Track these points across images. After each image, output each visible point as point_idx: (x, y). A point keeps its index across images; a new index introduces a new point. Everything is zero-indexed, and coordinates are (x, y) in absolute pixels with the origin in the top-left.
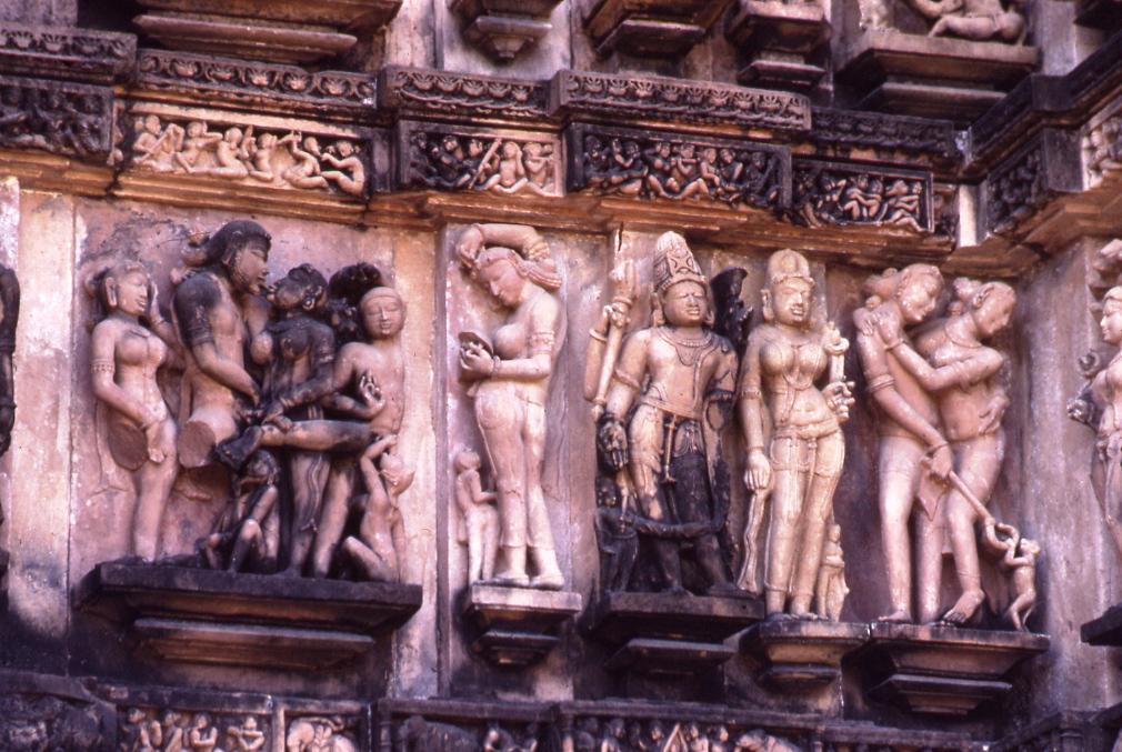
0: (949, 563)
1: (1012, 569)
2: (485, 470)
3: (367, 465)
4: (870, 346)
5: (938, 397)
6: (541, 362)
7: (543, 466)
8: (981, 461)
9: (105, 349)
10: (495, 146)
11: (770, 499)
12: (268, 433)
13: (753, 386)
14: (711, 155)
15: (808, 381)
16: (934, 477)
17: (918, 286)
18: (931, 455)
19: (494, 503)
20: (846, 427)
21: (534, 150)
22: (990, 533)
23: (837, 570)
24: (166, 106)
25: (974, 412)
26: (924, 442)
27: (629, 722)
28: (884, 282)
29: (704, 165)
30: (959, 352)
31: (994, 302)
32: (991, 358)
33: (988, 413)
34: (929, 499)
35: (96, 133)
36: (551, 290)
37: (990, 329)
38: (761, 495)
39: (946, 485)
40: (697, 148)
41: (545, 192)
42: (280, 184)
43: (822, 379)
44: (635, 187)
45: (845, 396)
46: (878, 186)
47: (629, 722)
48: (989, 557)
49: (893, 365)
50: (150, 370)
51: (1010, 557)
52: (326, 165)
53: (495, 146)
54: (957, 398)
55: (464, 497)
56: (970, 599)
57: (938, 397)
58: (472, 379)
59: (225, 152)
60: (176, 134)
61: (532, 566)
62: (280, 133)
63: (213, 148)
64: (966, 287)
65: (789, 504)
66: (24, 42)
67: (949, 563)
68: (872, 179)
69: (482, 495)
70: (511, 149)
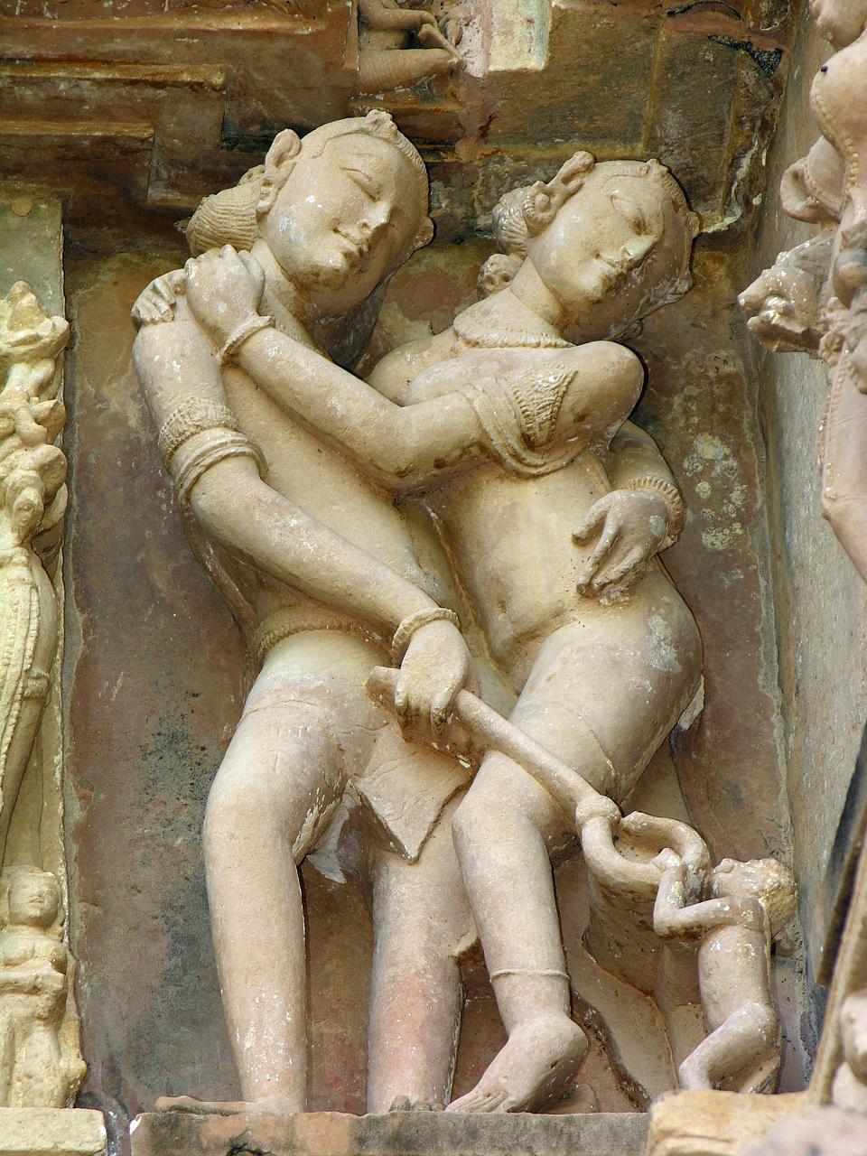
5: (431, 497)
8: (588, 678)
16: (411, 720)
18: (394, 658)
22: (595, 839)
23: (41, 1003)
25: (539, 533)
32: (603, 362)
33: (597, 528)
34: (398, 789)
37: (589, 279)
39: (449, 743)
45: (29, 443)
49: (258, 414)
51: (669, 911)
57: (431, 497)
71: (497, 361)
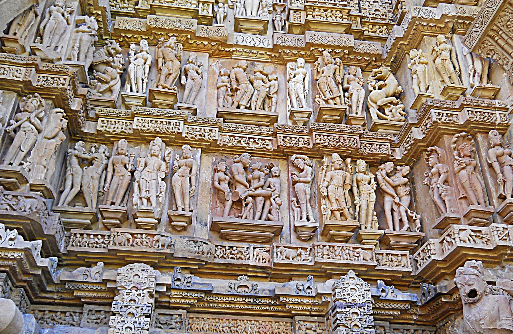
0: (401, 220)
1: (415, 220)
2: (298, 202)
3: (272, 200)
4: (379, 177)
6: (309, 179)
7: (310, 200)
8: (406, 201)
9: (216, 179)
10: (297, 139)
11: (360, 207)
12: (251, 193)
13: (355, 184)
14: (342, 138)
15: (367, 183)
16: (396, 203)
17: (389, 166)
19: (299, 207)
20: (375, 191)
21: (306, 140)
22: (409, 213)
25: (402, 191)
26: (393, 197)
27: (330, 247)
28: (382, 166)
29: (341, 140)
30: (399, 179)
31: (406, 169)
34: (395, 207)
35: (214, 136)
36: (311, 167)
37: (405, 174)
38: (358, 206)
40: (339, 137)
41: (308, 147)
42: (253, 148)
43: (369, 183)
44: (327, 144)
46: (378, 146)
47: (330, 247)
48: (409, 218)
49: (385, 181)
50: (227, 182)
52: (263, 144)
53: (297, 139)
54: (399, 188)
55: (293, 206)
56: (406, 226)
57: (395, 188)
58: (295, 183)
59: (242, 141)
61: (308, 219)
62: (254, 138)
63: (240, 142)
64: (399, 168)
65: (364, 207)
67: (401, 220)
68: (377, 145)
69: (297, 206)
70: (301, 139)
71: (399, 179)
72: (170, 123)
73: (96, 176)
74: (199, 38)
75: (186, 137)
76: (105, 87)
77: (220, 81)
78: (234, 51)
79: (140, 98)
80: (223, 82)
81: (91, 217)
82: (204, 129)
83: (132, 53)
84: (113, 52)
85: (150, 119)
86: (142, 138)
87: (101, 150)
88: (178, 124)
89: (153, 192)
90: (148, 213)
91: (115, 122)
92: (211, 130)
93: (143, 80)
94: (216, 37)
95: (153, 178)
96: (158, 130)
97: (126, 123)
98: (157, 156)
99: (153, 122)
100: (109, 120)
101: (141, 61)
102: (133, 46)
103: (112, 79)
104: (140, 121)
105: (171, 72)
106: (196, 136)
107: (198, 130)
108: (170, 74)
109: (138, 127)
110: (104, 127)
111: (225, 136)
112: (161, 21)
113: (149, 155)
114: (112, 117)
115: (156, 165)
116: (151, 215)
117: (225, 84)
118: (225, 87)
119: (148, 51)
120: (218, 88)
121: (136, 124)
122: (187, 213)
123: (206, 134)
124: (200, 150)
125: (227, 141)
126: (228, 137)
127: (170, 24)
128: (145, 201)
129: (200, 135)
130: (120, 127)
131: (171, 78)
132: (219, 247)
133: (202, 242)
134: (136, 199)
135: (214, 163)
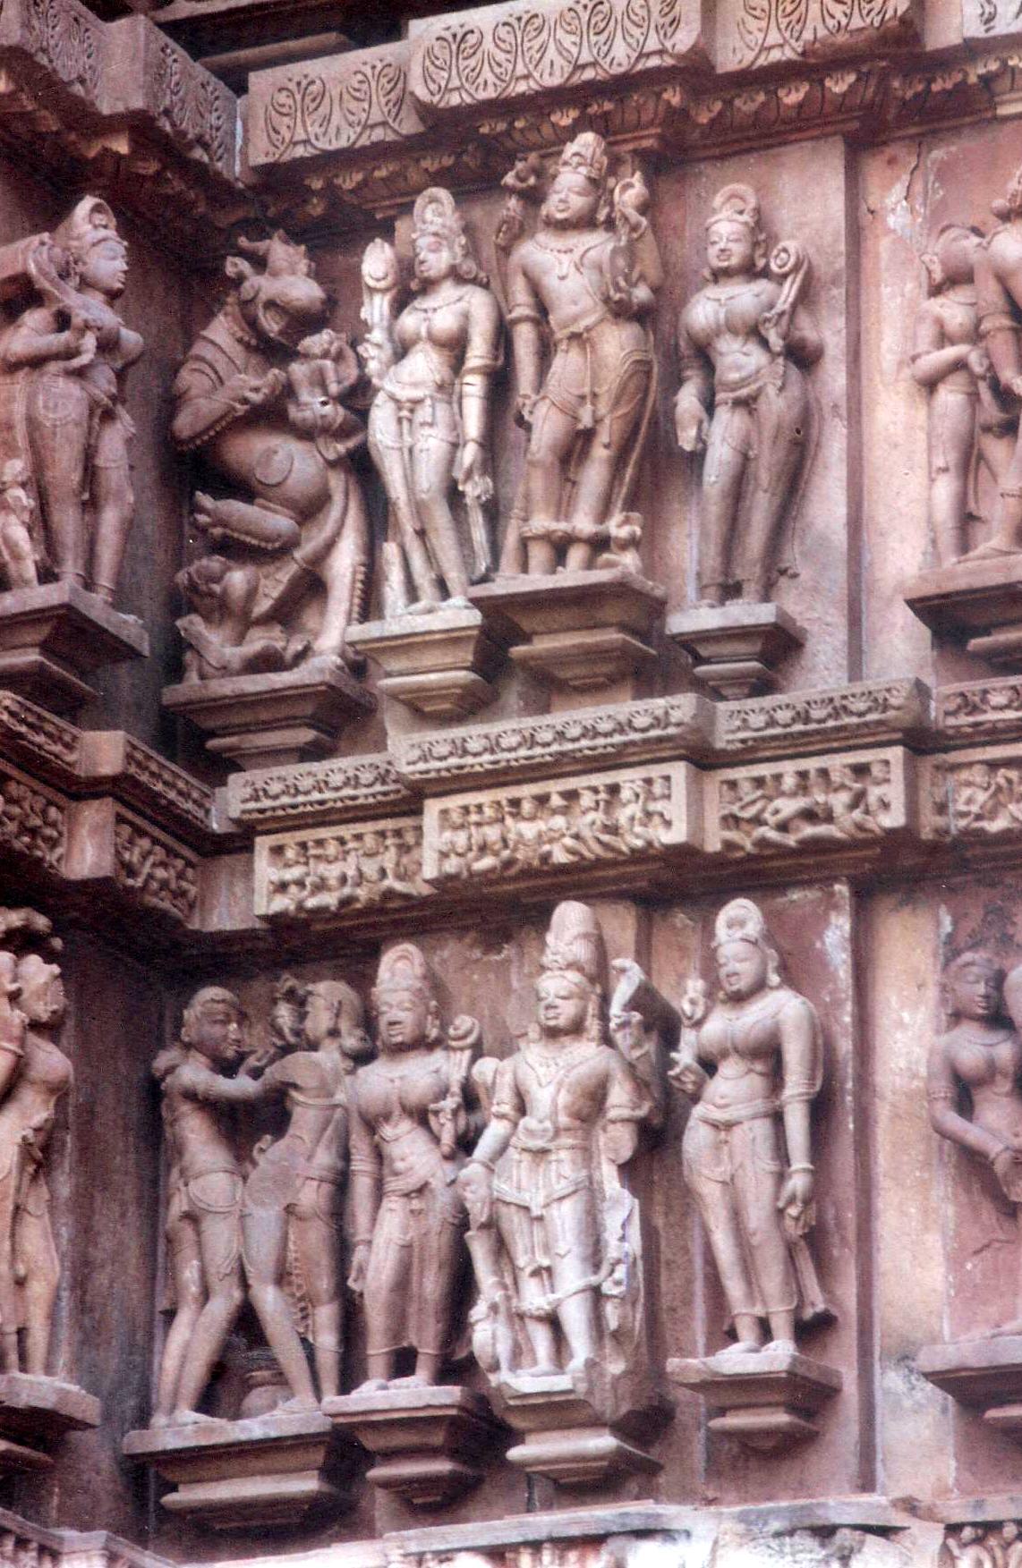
24: (988, 749)
60: (1009, 781)
66: (783, 716)
72: (614, 790)
73: (312, 1196)
74: (747, 79)
75: (729, 845)
76: (275, 584)
77: (927, 332)
78: (987, 80)
79: (451, 639)
80: (944, 338)
81: (318, 1456)
82: (824, 773)
83: (375, 309)
84: (272, 325)
85: (503, 794)
86: (498, 910)
87: (319, 1020)
88: (658, 789)
89: (572, 1276)
90: (559, 1412)
91: (342, 841)
92: (861, 770)
93: (454, 497)
94: (841, 38)
95: (562, 1187)
96: (560, 857)
97: (398, 833)
98: (576, 1029)
99: (527, 807)
100: (308, 835)
101: (424, 366)
102: (376, 262)
103: (310, 509)
104: (456, 817)
105: (586, 421)
106: (783, 827)
107: (789, 782)
108: (587, 436)
109: (452, 865)
110: (293, 889)
111: (964, 775)
112: (488, 44)
113: (534, 1031)
114: (324, 817)
115: (564, 1098)
116: (581, 1415)
117: (950, 353)
118: (959, 379)
119: (469, 266)
120: (930, 385)
121: (443, 846)
122: (780, 1353)
123: (839, 801)
124: (841, 889)
125: (975, 809)
126: (977, 774)
127: (543, 49)
128: (541, 1338)
129: (809, 815)
130: (370, 868)
131: (600, 454)
132: (967, 1533)
133: (855, 1527)
134: (487, 1334)
135: (951, 950)
